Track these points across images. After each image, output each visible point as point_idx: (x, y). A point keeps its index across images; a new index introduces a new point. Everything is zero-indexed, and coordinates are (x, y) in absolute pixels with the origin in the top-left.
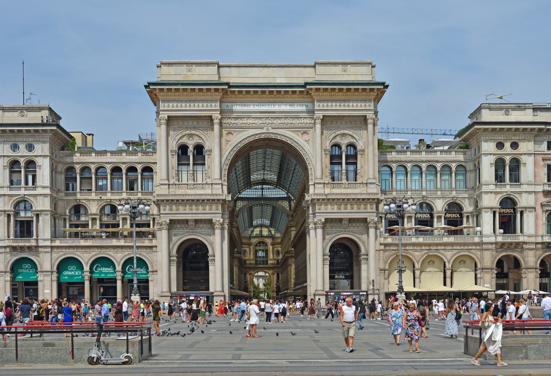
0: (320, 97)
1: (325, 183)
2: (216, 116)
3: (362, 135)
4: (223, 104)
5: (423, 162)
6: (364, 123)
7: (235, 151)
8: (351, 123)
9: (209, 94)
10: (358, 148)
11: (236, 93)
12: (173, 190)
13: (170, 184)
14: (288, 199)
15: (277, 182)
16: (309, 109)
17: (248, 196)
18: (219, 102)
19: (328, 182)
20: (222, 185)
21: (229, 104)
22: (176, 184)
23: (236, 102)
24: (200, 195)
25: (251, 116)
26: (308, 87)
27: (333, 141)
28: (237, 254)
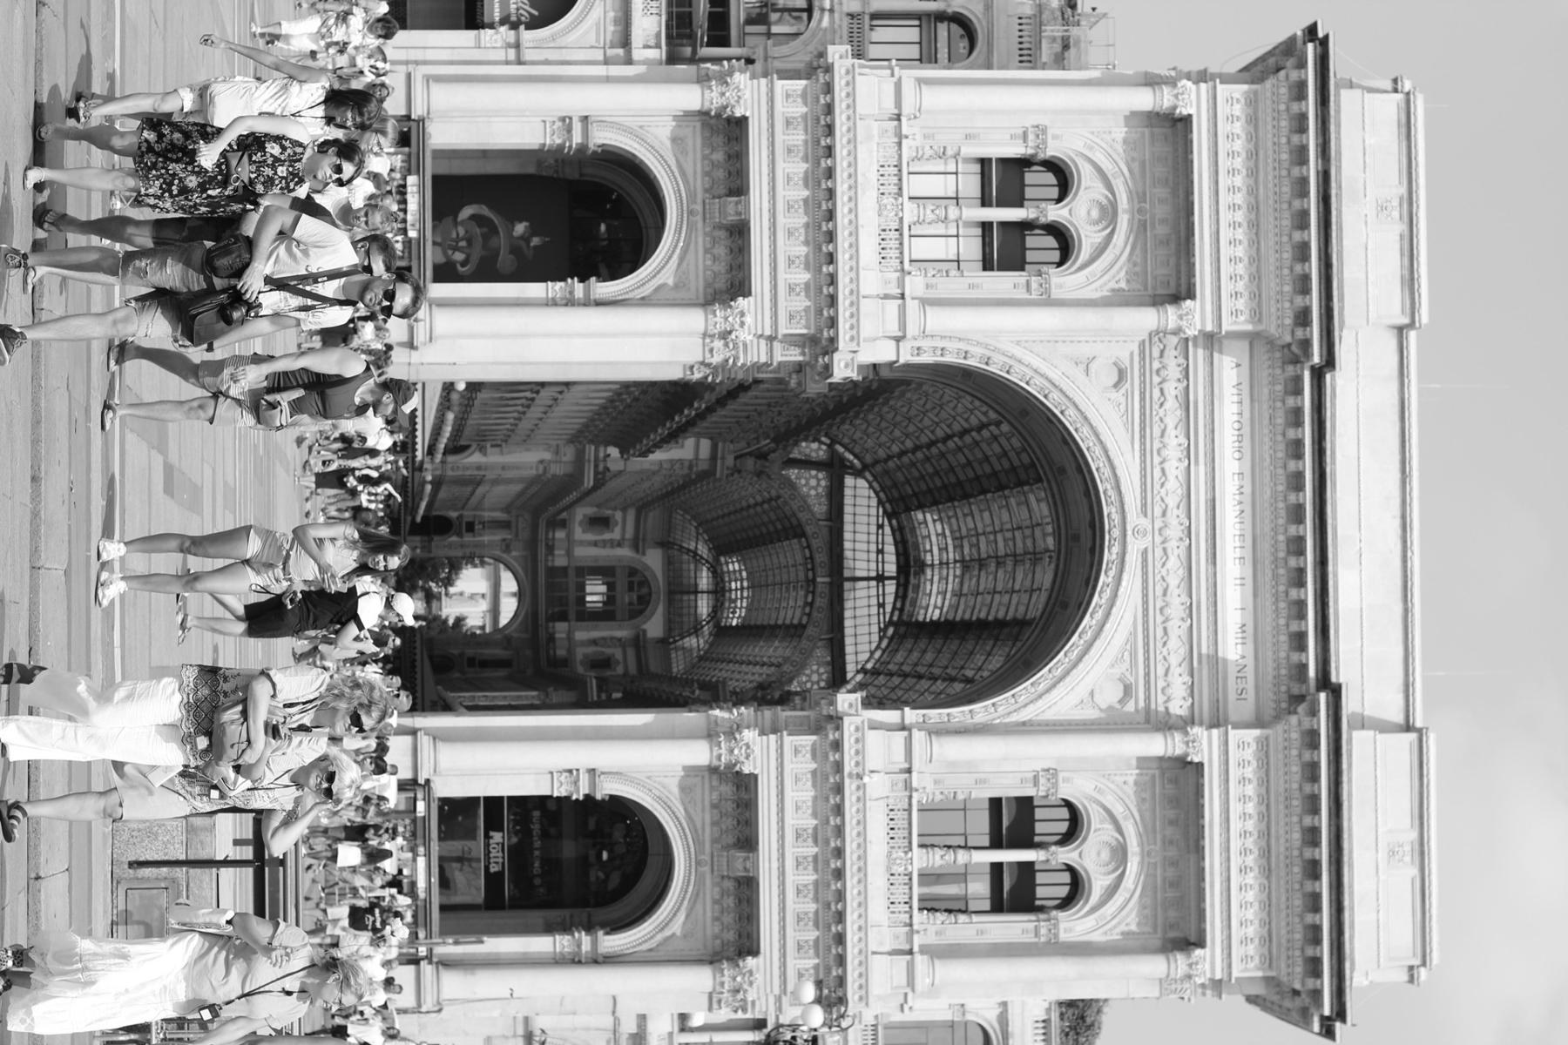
1: (909, 771)
2: (1195, 316)
4: (1245, 345)
8: (1172, 885)
9: (1287, 288)
12: (875, 132)
15: (908, 624)
16: (1231, 707)
17: (848, 518)
18: (1249, 327)
19: (915, 785)
22: (900, 144)
23: (1252, 400)
24: (855, 246)
26: (1323, 696)
28: (596, 473)
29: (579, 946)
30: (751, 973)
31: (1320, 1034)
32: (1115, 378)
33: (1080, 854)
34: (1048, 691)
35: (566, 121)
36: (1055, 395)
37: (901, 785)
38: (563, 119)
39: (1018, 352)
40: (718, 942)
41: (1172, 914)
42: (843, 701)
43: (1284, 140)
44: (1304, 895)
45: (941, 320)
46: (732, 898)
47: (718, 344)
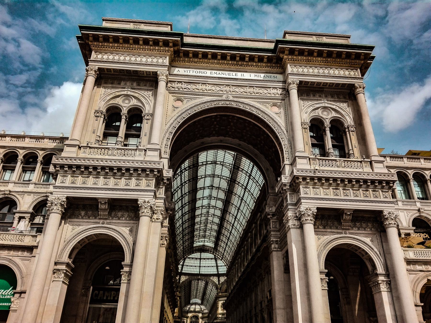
9: (157, 48)
10: (346, 125)
13: (82, 146)
14: (218, 275)
17: (189, 272)
21: (180, 69)
22: (90, 148)
25: (207, 81)
26: (279, 46)
27: (312, 114)
29: (383, 281)
30: (389, 213)
33: (326, 119)
34: (277, 123)
35: (55, 272)
36: (183, 115)
37: (313, 161)
38: (54, 273)
39: (168, 125)
40: (373, 229)
41: (341, 97)
42: (285, 180)
43: (111, 45)
44: (336, 58)
45: (156, 138)
46: (357, 224)
47: (155, 216)
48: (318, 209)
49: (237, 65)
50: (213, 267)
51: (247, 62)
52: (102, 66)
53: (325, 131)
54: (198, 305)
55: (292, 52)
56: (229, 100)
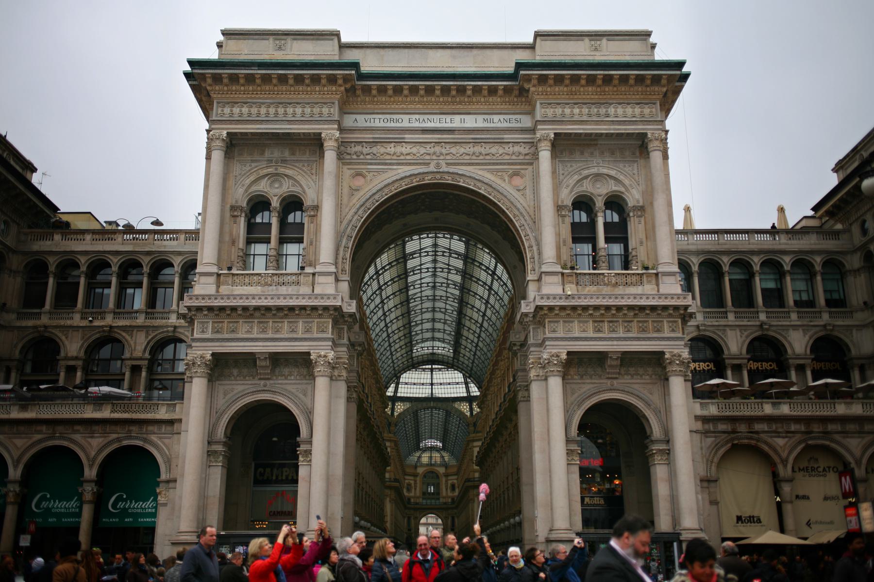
0: (546, 97)
1: (563, 274)
2: (330, 134)
3: (637, 178)
5: (753, 253)
6: (641, 153)
7: (369, 209)
9: (317, 89)
10: (631, 203)
11: (374, 92)
15: (454, 358)
16: (524, 126)
17: (411, 395)
20: (337, 280)
21: (358, 117)
22: (233, 275)
26: (522, 72)
27: (576, 190)
28: (394, 482)
31: (685, 82)
32: (360, 178)
34: (518, 210)
37: (570, 278)
38: (209, 455)
39: (345, 222)
40: (653, 376)
43: (242, 88)
48: (569, 353)
49: (453, 103)
50: (458, 383)
51: (469, 96)
52: (233, 129)
53: (596, 216)
54: (437, 451)
55: (543, 79)
56: (440, 172)
